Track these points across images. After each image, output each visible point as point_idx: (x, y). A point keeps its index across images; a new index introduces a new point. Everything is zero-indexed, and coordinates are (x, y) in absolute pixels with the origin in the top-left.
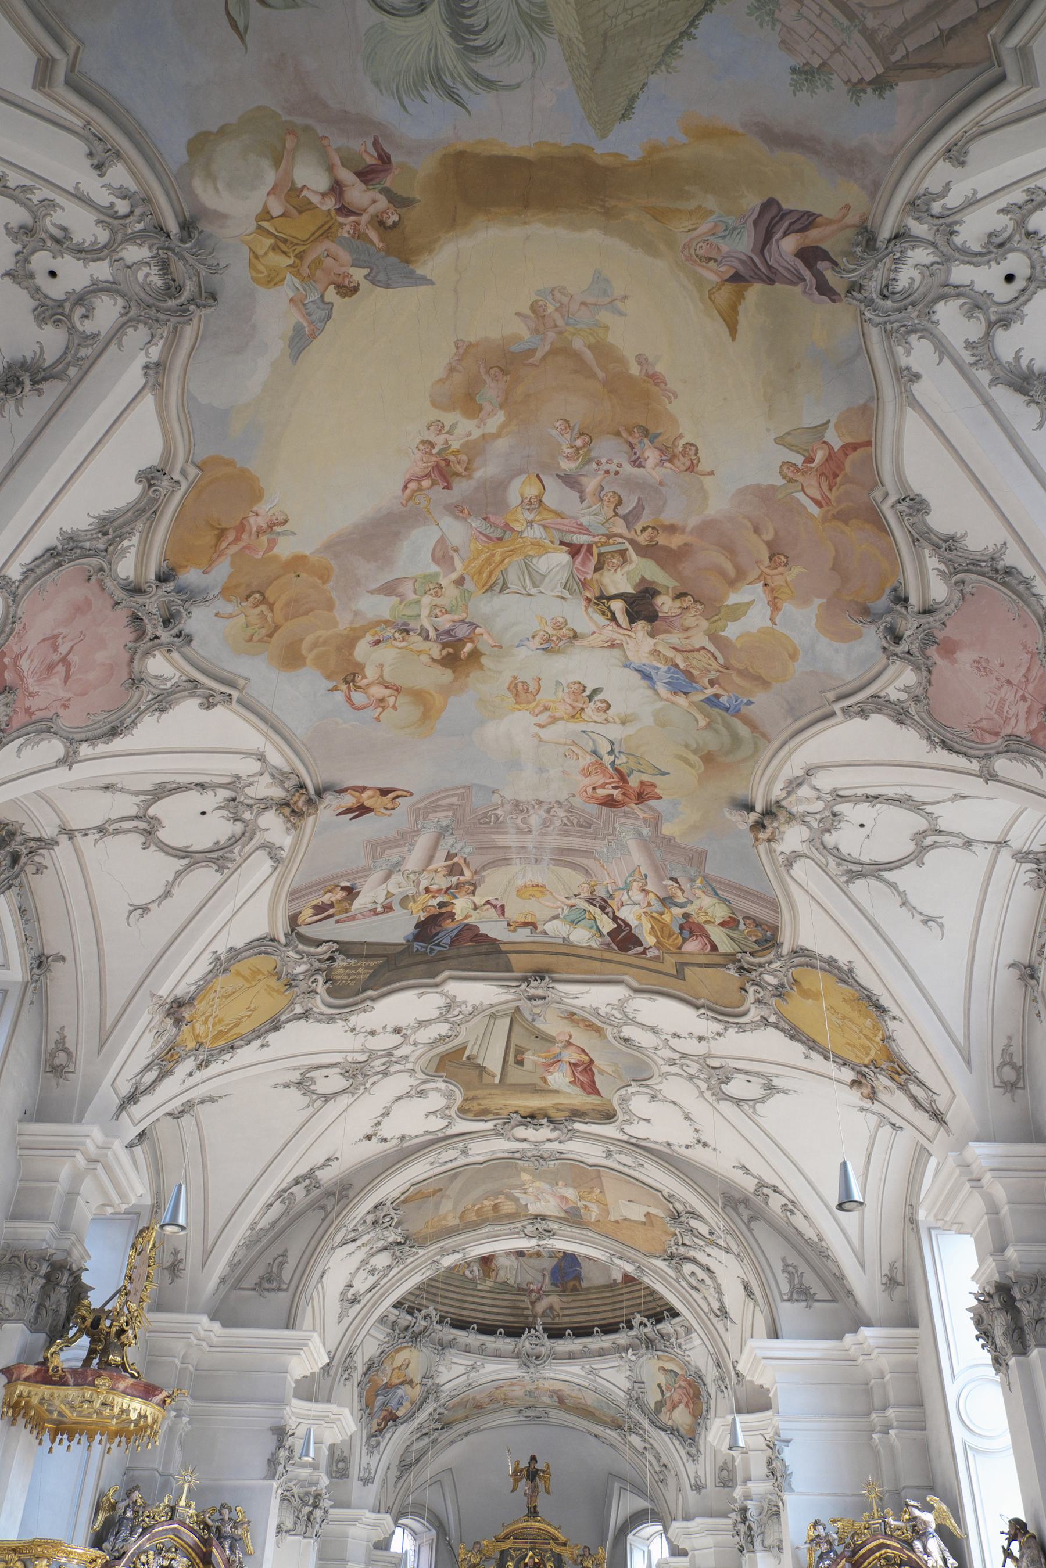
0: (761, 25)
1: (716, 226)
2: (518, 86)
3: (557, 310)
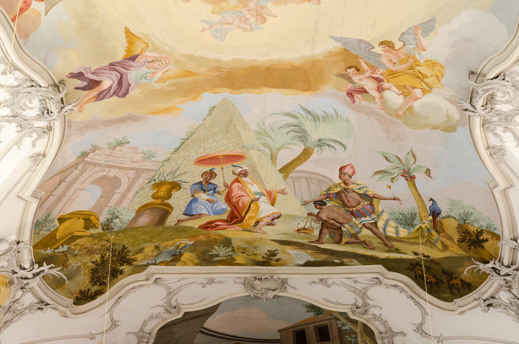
0: (149, 150)
1: (152, 77)
2: (272, 114)
3: (249, 20)
